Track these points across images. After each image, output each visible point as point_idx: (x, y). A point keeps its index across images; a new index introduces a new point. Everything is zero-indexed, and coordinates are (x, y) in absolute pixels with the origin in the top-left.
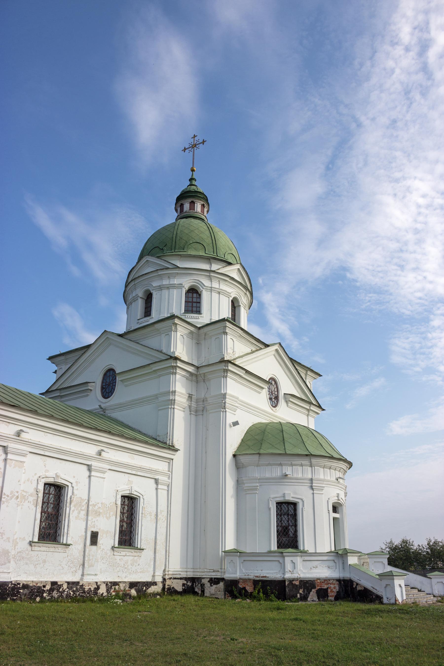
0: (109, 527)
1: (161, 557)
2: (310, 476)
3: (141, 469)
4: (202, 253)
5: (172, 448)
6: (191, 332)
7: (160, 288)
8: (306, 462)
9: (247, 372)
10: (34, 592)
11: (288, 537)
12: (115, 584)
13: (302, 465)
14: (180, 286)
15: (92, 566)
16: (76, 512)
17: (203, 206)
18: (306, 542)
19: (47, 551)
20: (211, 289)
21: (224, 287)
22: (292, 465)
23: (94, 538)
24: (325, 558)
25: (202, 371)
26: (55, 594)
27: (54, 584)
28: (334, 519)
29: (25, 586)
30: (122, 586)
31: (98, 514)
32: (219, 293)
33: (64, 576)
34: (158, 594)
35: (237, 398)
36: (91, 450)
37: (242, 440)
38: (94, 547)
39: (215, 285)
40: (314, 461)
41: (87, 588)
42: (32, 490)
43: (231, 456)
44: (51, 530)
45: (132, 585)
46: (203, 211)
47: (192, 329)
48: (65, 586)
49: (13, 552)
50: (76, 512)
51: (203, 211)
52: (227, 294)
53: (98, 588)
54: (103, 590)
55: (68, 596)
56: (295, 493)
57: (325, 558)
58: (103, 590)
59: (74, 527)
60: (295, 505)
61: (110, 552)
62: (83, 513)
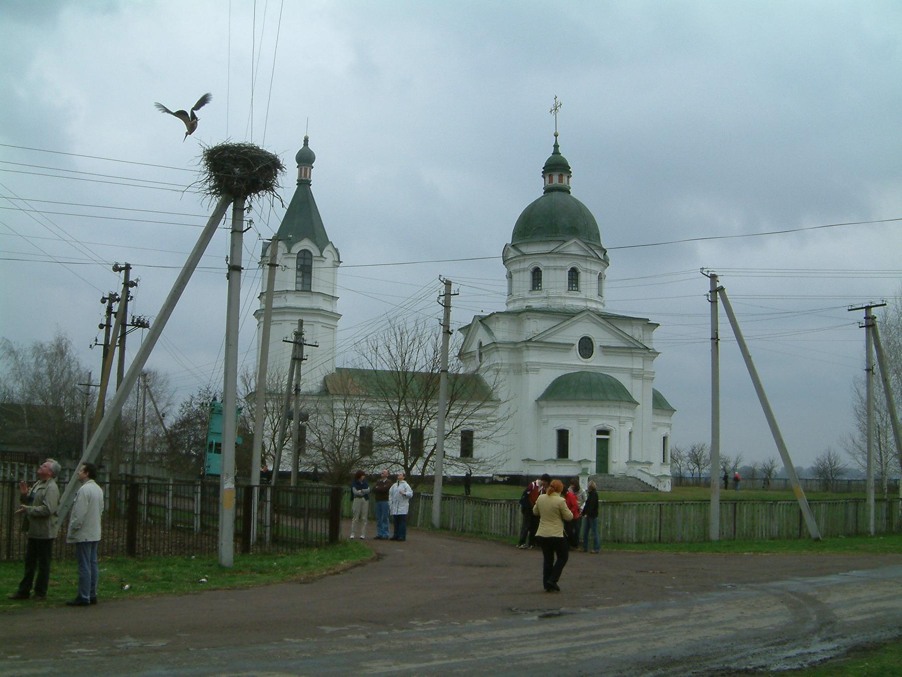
11: (563, 451)
14: (524, 270)
17: (561, 176)
18: (573, 453)
20: (547, 268)
21: (560, 263)
28: (598, 439)
37: (547, 390)
46: (561, 180)
51: (561, 180)
60: (568, 431)
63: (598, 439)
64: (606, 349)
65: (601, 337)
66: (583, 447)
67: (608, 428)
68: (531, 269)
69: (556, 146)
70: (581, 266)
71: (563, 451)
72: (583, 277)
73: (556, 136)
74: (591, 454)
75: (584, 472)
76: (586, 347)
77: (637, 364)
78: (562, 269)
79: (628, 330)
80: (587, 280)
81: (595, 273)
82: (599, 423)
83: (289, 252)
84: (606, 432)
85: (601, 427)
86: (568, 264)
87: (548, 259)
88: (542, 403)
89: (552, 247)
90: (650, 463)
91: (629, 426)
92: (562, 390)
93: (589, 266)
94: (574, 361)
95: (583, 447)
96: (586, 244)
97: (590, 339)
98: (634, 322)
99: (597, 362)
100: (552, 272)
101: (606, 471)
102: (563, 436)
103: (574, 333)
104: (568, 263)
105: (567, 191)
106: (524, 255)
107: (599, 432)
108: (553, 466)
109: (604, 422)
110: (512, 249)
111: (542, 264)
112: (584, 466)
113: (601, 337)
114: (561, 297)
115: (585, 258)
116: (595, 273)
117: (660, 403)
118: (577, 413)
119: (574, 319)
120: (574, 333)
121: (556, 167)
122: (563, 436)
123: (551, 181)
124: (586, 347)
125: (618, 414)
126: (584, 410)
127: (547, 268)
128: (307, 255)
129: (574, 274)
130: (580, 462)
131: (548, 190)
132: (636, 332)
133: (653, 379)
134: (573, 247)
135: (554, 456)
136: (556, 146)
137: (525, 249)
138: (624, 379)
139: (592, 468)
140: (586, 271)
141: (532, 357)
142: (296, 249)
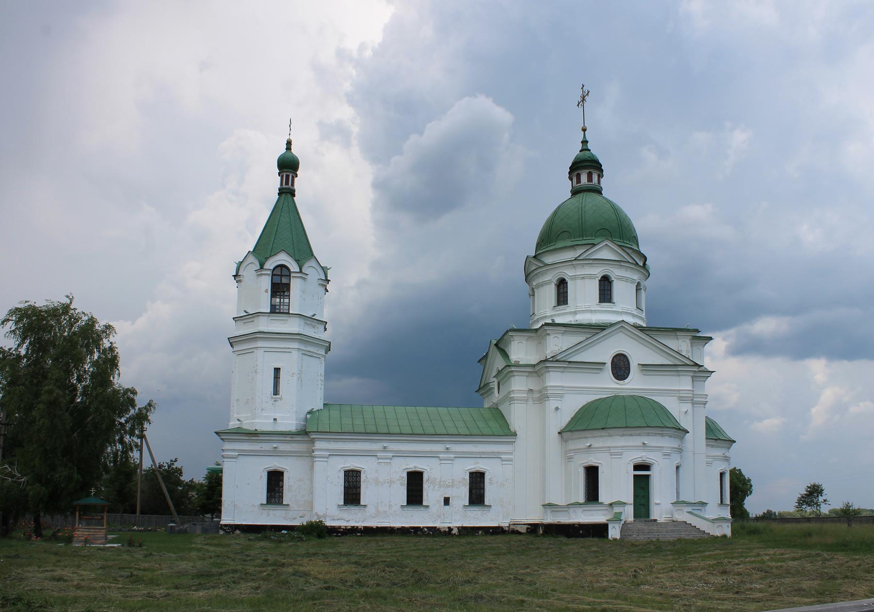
0: (462, 494)
5: (515, 434)
7: (540, 286)
14: (549, 282)
16: (432, 487)
20: (574, 278)
23: (447, 501)
25: (537, 368)
28: (635, 476)
38: (447, 507)
40: (611, 431)
46: (590, 179)
50: (432, 487)
51: (590, 179)
52: (591, 277)
54: (455, 531)
58: (455, 531)
59: (431, 494)
62: (437, 487)
63: (635, 476)
64: (645, 368)
65: (639, 354)
66: (617, 487)
67: (649, 461)
69: (585, 142)
70: (615, 273)
71: (592, 494)
73: (584, 130)
74: (627, 493)
75: (617, 518)
77: (684, 384)
78: (591, 277)
79: (673, 343)
80: (622, 291)
81: (633, 281)
82: (640, 456)
83: (262, 267)
84: (647, 467)
85: (639, 461)
86: (599, 271)
87: (574, 266)
88: (565, 435)
89: (579, 252)
90: (704, 504)
91: (676, 460)
92: (590, 420)
94: (606, 384)
95: (617, 487)
96: (620, 246)
98: (679, 333)
100: (579, 282)
101: (647, 514)
102: (592, 473)
105: (599, 192)
106: (547, 265)
107: (637, 467)
108: (579, 510)
109: (644, 454)
110: (533, 261)
111: (568, 273)
112: (617, 509)
113: (639, 354)
114: (591, 311)
115: (618, 263)
116: (633, 281)
117: (715, 435)
118: (609, 445)
119: (605, 332)
120: (603, 352)
121: (586, 165)
122: (592, 473)
123: (579, 181)
124: (620, 367)
126: (618, 441)
127: (574, 278)
128: (285, 272)
129: (606, 283)
130: (611, 505)
131: (575, 192)
132: (682, 345)
133: (705, 403)
134: (606, 251)
135: (581, 498)
136: (585, 142)
137: (549, 259)
138: (671, 405)
139: (629, 514)
140: (621, 278)
141: (554, 379)
142: (271, 264)
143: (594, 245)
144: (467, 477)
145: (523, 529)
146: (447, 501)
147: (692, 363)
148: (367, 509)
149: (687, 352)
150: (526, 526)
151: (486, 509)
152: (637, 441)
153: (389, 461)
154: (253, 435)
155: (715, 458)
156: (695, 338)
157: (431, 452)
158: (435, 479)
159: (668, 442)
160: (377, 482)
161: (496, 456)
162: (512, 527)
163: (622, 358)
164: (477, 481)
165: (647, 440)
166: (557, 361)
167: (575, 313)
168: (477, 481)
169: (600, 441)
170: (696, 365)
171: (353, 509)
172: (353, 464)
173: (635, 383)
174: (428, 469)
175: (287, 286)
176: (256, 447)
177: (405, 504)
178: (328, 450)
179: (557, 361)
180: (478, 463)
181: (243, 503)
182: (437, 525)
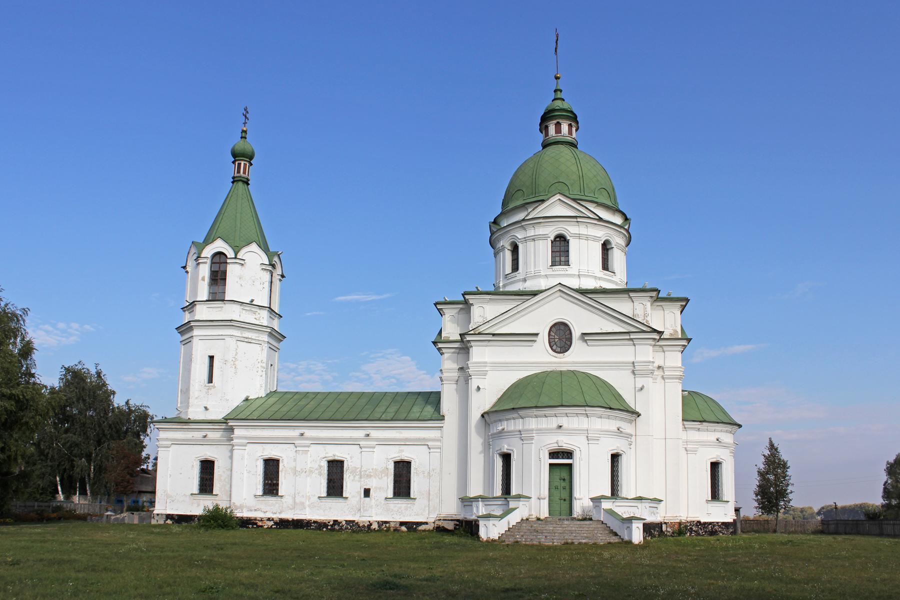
0: (385, 484)
1: (431, 505)
2: (521, 428)
3: (407, 440)
4: (519, 202)
5: (442, 418)
6: (461, 309)
8: (515, 415)
9: (494, 335)
10: (321, 525)
12: (386, 522)
13: (514, 419)
15: (366, 510)
16: (352, 477)
19: (335, 502)
20: (526, 240)
22: (507, 420)
23: (367, 493)
24: (500, 503)
26: (336, 527)
27: (335, 521)
28: (550, 464)
29: (315, 522)
30: (392, 525)
31: (369, 476)
32: (534, 240)
33: (342, 517)
34: (429, 531)
35: (486, 363)
36: (361, 434)
38: (367, 499)
39: (531, 232)
40: (522, 413)
41: (361, 525)
42: (317, 466)
43: (480, 415)
44: (335, 488)
45: (402, 524)
47: (461, 306)
48: (344, 523)
49: (307, 503)
52: (544, 237)
53: (371, 524)
54: (375, 526)
55: (346, 528)
56: (509, 445)
57: (500, 503)
59: (351, 486)
61: (383, 502)
62: (357, 477)
63: (550, 464)
65: (581, 320)
67: (566, 447)
68: (508, 246)
70: (570, 230)
72: (574, 246)
76: (561, 337)
79: (623, 306)
84: (569, 454)
85: (554, 447)
86: (551, 231)
93: (582, 230)
94: (540, 357)
97: (565, 325)
98: (632, 294)
99: (578, 356)
100: (531, 244)
103: (538, 319)
104: (551, 229)
107: (553, 454)
113: (581, 320)
116: (596, 239)
120: (538, 319)
123: (547, 134)
124: (561, 337)
125: (585, 426)
127: (526, 240)
140: (579, 236)
143: (543, 201)
144: (391, 467)
145: (450, 526)
146: (367, 493)
147: (649, 330)
148: (284, 500)
149: (645, 315)
150: (453, 523)
151: (410, 501)
152: (553, 423)
153: (307, 449)
154: (188, 422)
155: (703, 444)
156: (658, 299)
157: (351, 439)
158: (356, 468)
159: (601, 422)
160: (295, 472)
161: (423, 442)
162: (437, 523)
163: (562, 327)
164: (402, 470)
165: (564, 421)
166: (479, 334)
167: (525, 280)
168: (402, 470)
169: (511, 425)
170: (655, 331)
171: (271, 500)
172: (272, 452)
173: (578, 356)
174: (349, 459)
175: (225, 273)
176: (188, 435)
177: (325, 494)
178: (246, 438)
179: (479, 334)
180: (402, 451)
181: (175, 492)
182: (356, 518)
